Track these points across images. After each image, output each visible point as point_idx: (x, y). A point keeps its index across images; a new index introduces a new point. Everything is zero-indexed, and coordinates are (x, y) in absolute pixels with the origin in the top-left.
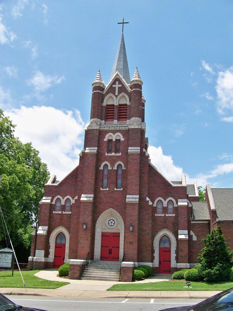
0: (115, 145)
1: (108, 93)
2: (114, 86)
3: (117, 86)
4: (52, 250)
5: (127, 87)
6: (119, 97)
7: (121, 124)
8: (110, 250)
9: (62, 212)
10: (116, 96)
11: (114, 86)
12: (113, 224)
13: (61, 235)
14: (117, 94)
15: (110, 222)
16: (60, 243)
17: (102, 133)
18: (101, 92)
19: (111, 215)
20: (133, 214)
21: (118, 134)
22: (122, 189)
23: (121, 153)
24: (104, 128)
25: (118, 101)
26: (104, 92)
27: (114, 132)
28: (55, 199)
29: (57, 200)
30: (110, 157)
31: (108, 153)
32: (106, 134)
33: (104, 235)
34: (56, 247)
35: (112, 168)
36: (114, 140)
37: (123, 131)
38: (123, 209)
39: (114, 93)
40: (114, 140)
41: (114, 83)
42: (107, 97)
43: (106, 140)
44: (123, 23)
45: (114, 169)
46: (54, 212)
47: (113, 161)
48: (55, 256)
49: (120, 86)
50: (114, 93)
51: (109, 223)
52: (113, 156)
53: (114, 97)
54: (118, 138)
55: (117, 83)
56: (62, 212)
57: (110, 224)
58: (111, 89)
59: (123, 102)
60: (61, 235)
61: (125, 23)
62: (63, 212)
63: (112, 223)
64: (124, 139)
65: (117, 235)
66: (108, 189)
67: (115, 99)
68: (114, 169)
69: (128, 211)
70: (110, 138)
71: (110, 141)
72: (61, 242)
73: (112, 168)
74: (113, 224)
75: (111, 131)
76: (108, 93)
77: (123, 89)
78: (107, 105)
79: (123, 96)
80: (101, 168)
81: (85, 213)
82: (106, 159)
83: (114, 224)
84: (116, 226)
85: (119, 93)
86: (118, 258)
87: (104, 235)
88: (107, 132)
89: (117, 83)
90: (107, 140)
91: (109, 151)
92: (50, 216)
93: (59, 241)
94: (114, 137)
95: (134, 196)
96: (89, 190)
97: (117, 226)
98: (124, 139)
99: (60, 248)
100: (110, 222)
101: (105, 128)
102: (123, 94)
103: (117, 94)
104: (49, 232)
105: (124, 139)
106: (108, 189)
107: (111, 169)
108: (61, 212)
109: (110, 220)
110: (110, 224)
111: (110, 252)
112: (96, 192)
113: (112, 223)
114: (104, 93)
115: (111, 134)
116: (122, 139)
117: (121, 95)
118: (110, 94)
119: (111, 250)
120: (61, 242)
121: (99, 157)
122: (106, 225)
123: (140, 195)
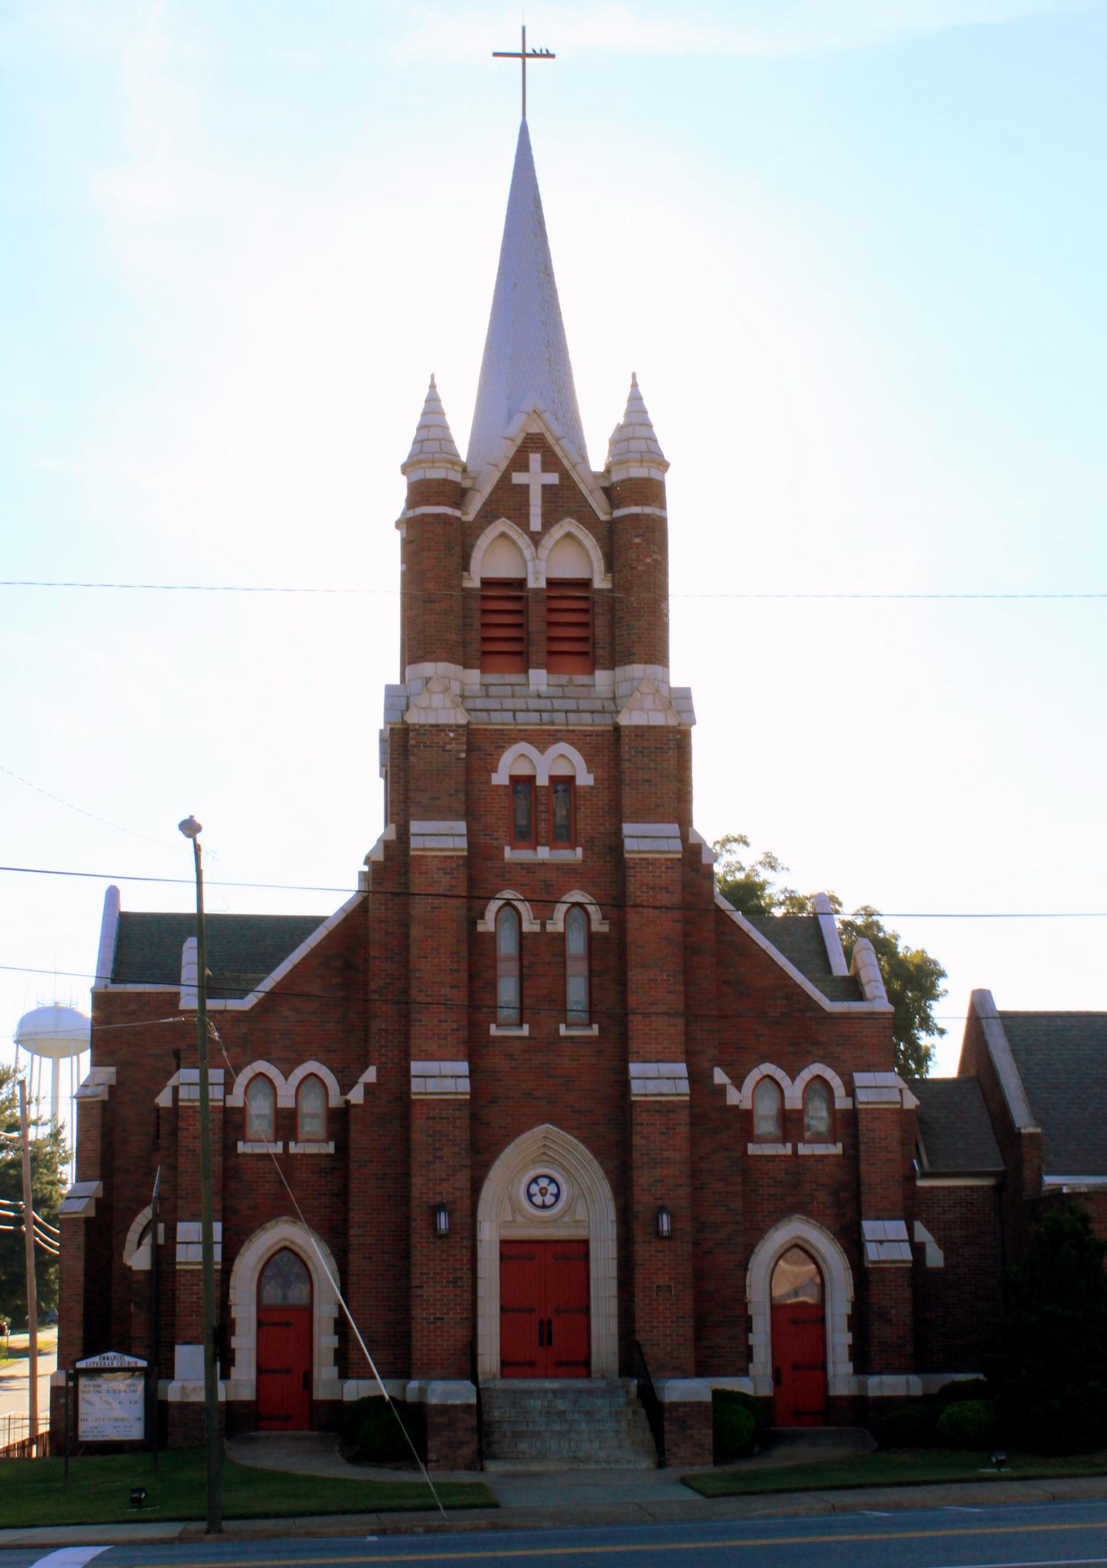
0: (537, 808)
1: (488, 515)
2: (518, 478)
3: (536, 478)
4: (244, 1342)
5: (557, 440)
6: (548, 542)
7: (569, 691)
8: (541, 1322)
9: (286, 1147)
10: (536, 539)
11: (518, 478)
12: (549, 1200)
13: (286, 1263)
14: (536, 524)
15: (534, 1189)
16: (279, 1301)
17: (480, 744)
18: (457, 513)
19: (544, 1156)
20: (665, 1154)
21: (562, 747)
22: (595, 1030)
23: (579, 851)
24: (484, 714)
25: (543, 564)
26: (471, 513)
27: (543, 739)
28: (242, 1080)
29: (303, 1087)
30: (529, 868)
31: (513, 848)
32: (502, 748)
33: (512, 1251)
34: (260, 1324)
35: (543, 925)
36: (542, 781)
37: (587, 734)
38: (614, 1131)
39: (521, 518)
40: (542, 781)
41: (519, 462)
42: (483, 543)
43: (500, 778)
44: (524, 55)
45: (549, 928)
46: (242, 1147)
47: (543, 891)
48: (260, 1371)
49: (553, 478)
50: (521, 518)
51: (530, 1196)
52: (543, 864)
53: (524, 542)
54: (562, 770)
55: (535, 459)
56: (286, 1147)
57: (538, 1200)
58: (508, 501)
59: (569, 567)
60: (286, 1263)
61: (535, 55)
62: (292, 1144)
63: (543, 1192)
64: (592, 776)
65: (580, 1249)
66: (525, 1031)
67: (528, 551)
68: (549, 928)
69: (643, 1142)
70: (523, 770)
71: (523, 783)
72: (285, 1296)
73: (543, 925)
74: (549, 1200)
75: (527, 736)
76: (488, 515)
77: (564, 499)
78: (487, 583)
79: (569, 535)
80: (487, 925)
81: (438, 1154)
82: (510, 875)
83: (557, 1196)
84: (565, 1212)
85: (549, 520)
86: (587, 1363)
87: (510, 1249)
88: (503, 739)
89: (535, 459)
90: (506, 781)
91: (527, 837)
92: (225, 1170)
93: (273, 1294)
94: (547, 764)
95: (667, 1068)
96: (442, 1042)
97: (570, 1208)
98: (592, 776)
99: (284, 1326)
100: (534, 1189)
101: (496, 717)
102: (569, 525)
103: (536, 524)
104: (231, 1252)
105: (596, 779)
106: (525, 1031)
107: (537, 928)
108: (280, 1144)
109: (535, 1180)
110: (538, 1200)
111: (545, 1336)
112: (474, 1047)
113: (543, 1192)
114: (470, 517)
115: (523, 747)
116: (585, 779)
117: (557, 532)
118: (502, 525)
119: (550, 1322)
120: (285, 1296)
121: (477, 874)
122: (516, 1208)
123: (689, 1057)
